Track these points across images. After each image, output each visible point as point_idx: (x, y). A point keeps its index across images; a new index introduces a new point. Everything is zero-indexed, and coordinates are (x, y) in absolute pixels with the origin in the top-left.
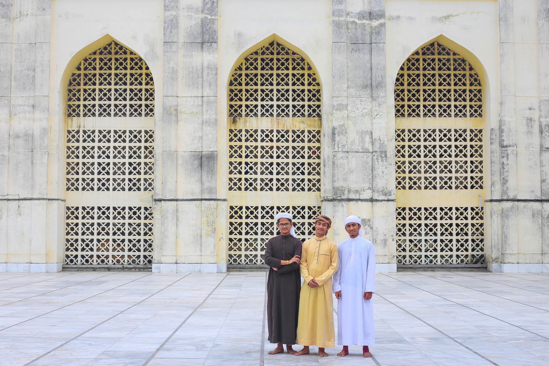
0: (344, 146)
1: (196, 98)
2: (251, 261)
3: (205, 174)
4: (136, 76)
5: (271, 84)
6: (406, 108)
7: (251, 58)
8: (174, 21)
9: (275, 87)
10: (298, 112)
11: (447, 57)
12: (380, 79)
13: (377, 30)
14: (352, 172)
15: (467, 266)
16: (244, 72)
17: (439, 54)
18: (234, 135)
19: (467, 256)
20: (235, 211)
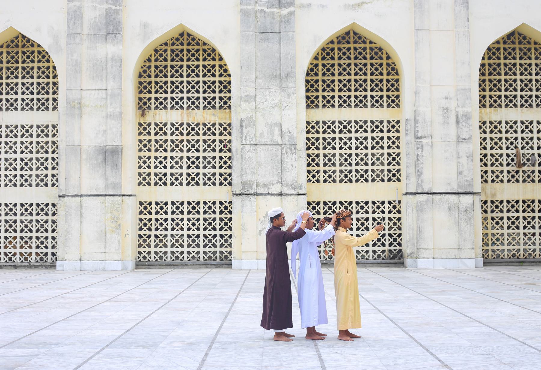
0: (252, 138)
1: (100, 91)
2: (161, 257)
3: (109, 168)
4: (43, 69)
5: (181, 76)
6: (320, 99)
7: (161, 50)
8: (78, 12)
9: (185, 79)
10: (209, 104)
11: (363, 46)
12: (290, 69)
13: (286, 19)
14: (260, 165)
15: (383, 261)
16: (153, 64)
17: (355, 42)
18: (143, 128)
19: (384, 251)
20: (144, 207)
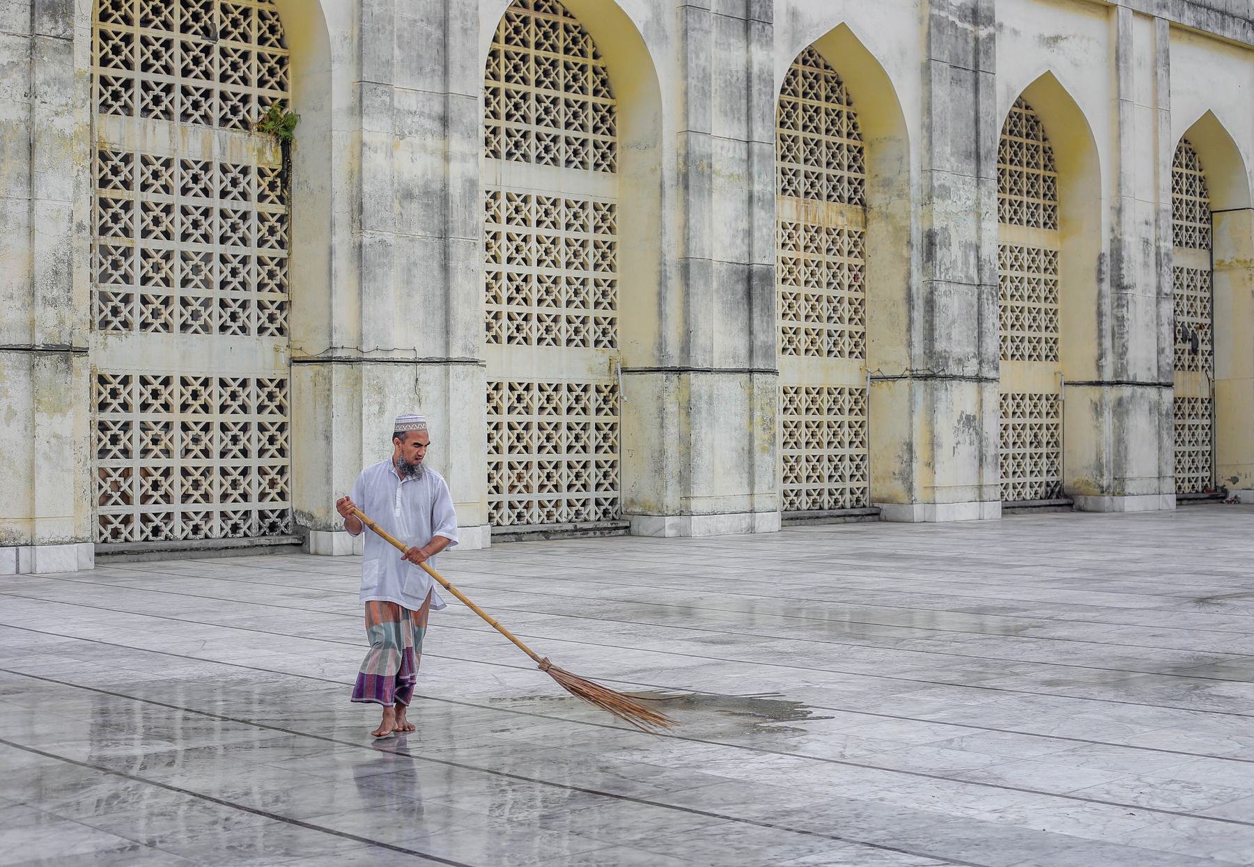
0: (947, 269)
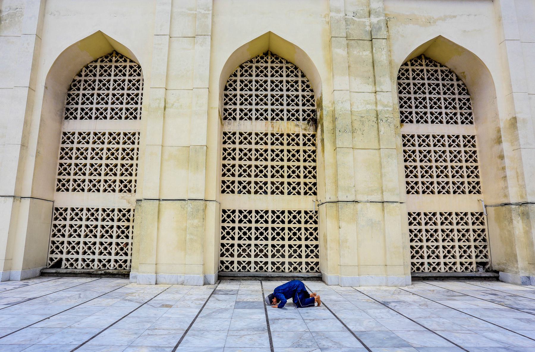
2: (244, 268)
7: (246, 66)
